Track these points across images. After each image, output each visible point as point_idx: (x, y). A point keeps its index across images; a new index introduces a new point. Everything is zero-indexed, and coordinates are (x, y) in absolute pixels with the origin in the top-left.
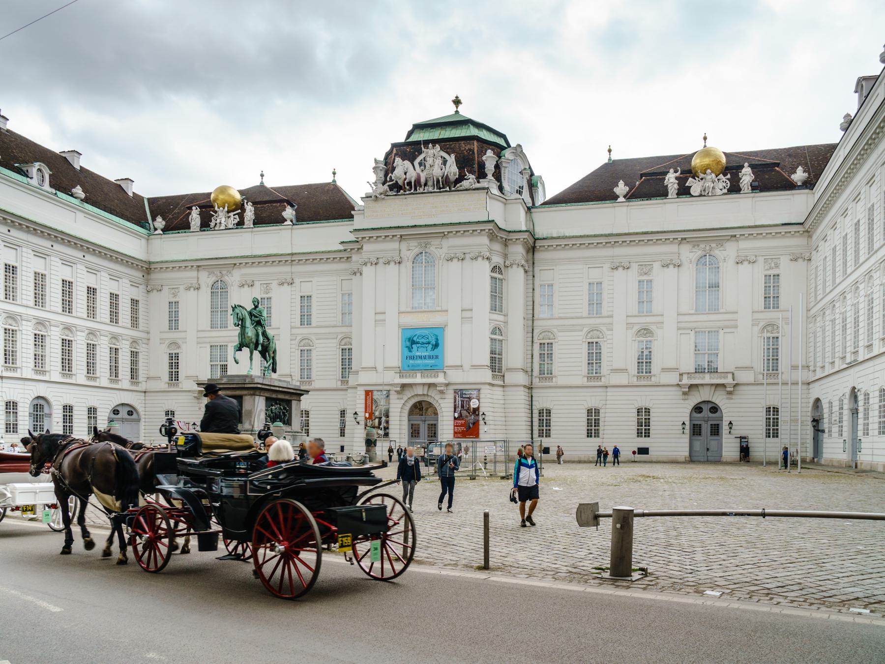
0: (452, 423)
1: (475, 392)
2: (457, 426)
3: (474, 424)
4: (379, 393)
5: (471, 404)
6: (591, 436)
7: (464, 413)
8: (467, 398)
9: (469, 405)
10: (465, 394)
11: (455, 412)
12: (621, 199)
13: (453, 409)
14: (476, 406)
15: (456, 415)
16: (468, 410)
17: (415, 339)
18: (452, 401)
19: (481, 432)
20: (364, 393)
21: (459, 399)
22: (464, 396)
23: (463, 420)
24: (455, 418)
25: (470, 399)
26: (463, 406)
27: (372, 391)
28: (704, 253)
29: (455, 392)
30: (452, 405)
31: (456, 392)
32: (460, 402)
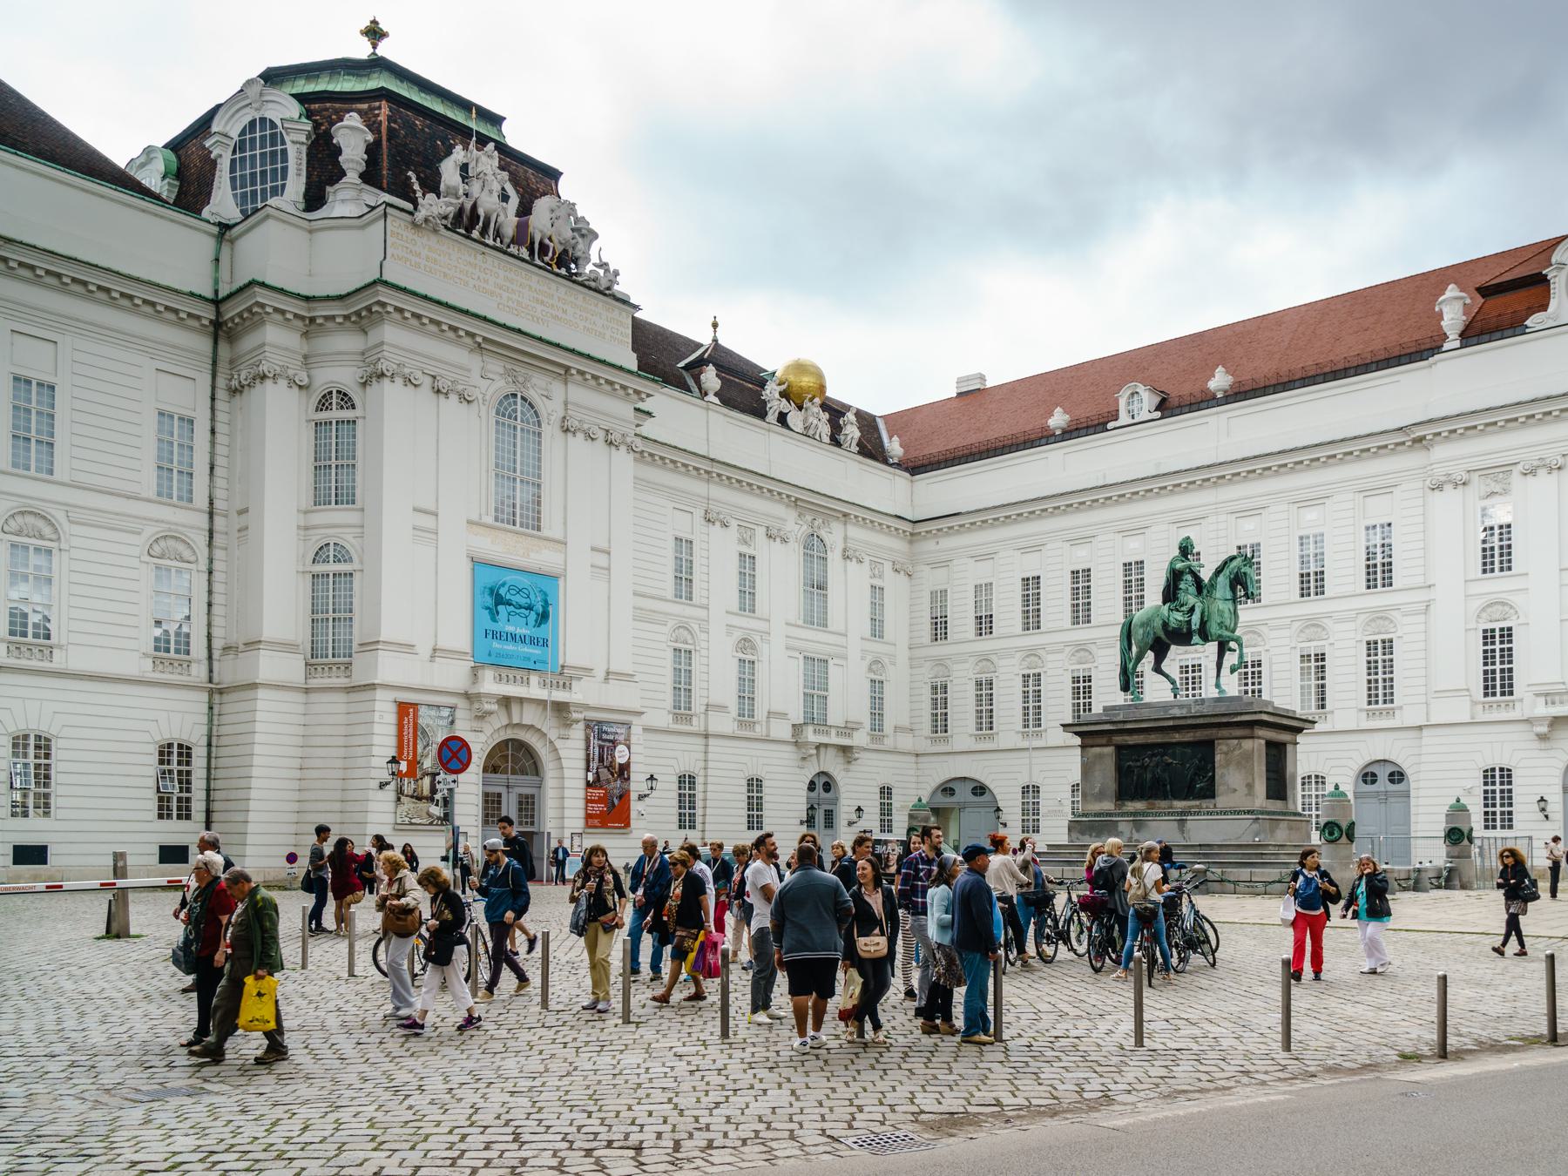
0: (581, 794)
1: (623, 731)
2: (592, 801)
3: (621, 797)
4: (433, 713)
5: (617, 754)
6: (169, 816)
7: (605, 774)
8: (610, 741)
9: (613, 757)
10: (606, 733)
11: (588, 770)
12: (711, 398)
13: (582, 764)
14: (623, 761)
15: (591, 777)
16: (610, 768)
17: (502, 591)
18: (582, 745)
19: (633, 814)
20: (393, 708)
21: (594, 742)
22: (604, 736)
23: (601, 788)
24: (588, 782)
25: (614, 743)
26: (601, 760)
27: (415, 706)
28: (810, 531)
29: (587, 727)
30: (582, 754)
31: (589, 724)
32: (597, 749)
